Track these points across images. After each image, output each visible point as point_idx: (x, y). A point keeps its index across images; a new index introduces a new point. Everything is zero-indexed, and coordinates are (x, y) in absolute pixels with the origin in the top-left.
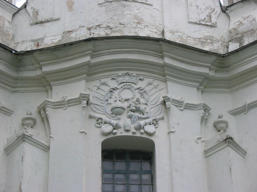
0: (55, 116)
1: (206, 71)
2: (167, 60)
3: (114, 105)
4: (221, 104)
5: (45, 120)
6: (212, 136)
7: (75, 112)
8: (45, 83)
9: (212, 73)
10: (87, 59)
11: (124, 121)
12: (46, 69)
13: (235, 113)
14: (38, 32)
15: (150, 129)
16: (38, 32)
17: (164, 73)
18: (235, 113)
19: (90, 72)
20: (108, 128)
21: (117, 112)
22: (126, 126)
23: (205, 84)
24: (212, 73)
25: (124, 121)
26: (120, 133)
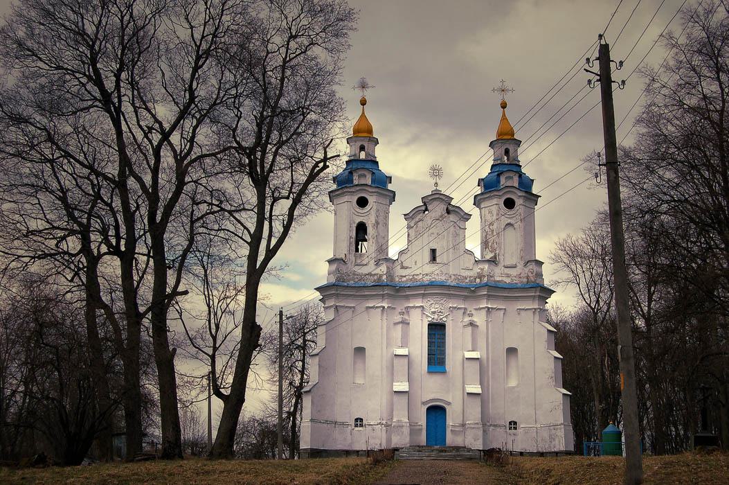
0: (413, 312)
1: (466, 294)
2: (452, 292)
3: (433, 310)
4: (471, 307)
5: (408, 312)
6: (467, 319)
7: (419, 311)
8: (407, 297)
9: (468, 294)
10: (423, 292)
11: (436, 317)
12: (407, 293)
13: (476, 309)
14: (404, 272)
15: (445, 319)
16: (404, 272)
17: (450, 296)
18: (476, 309)
19: (424, 296)
20: (430, 319)
21: (434, 313)
22: (436, 319)
23: (466, 298)
24: (468, 294)
25: (436, 317)
26: (435, 321)
